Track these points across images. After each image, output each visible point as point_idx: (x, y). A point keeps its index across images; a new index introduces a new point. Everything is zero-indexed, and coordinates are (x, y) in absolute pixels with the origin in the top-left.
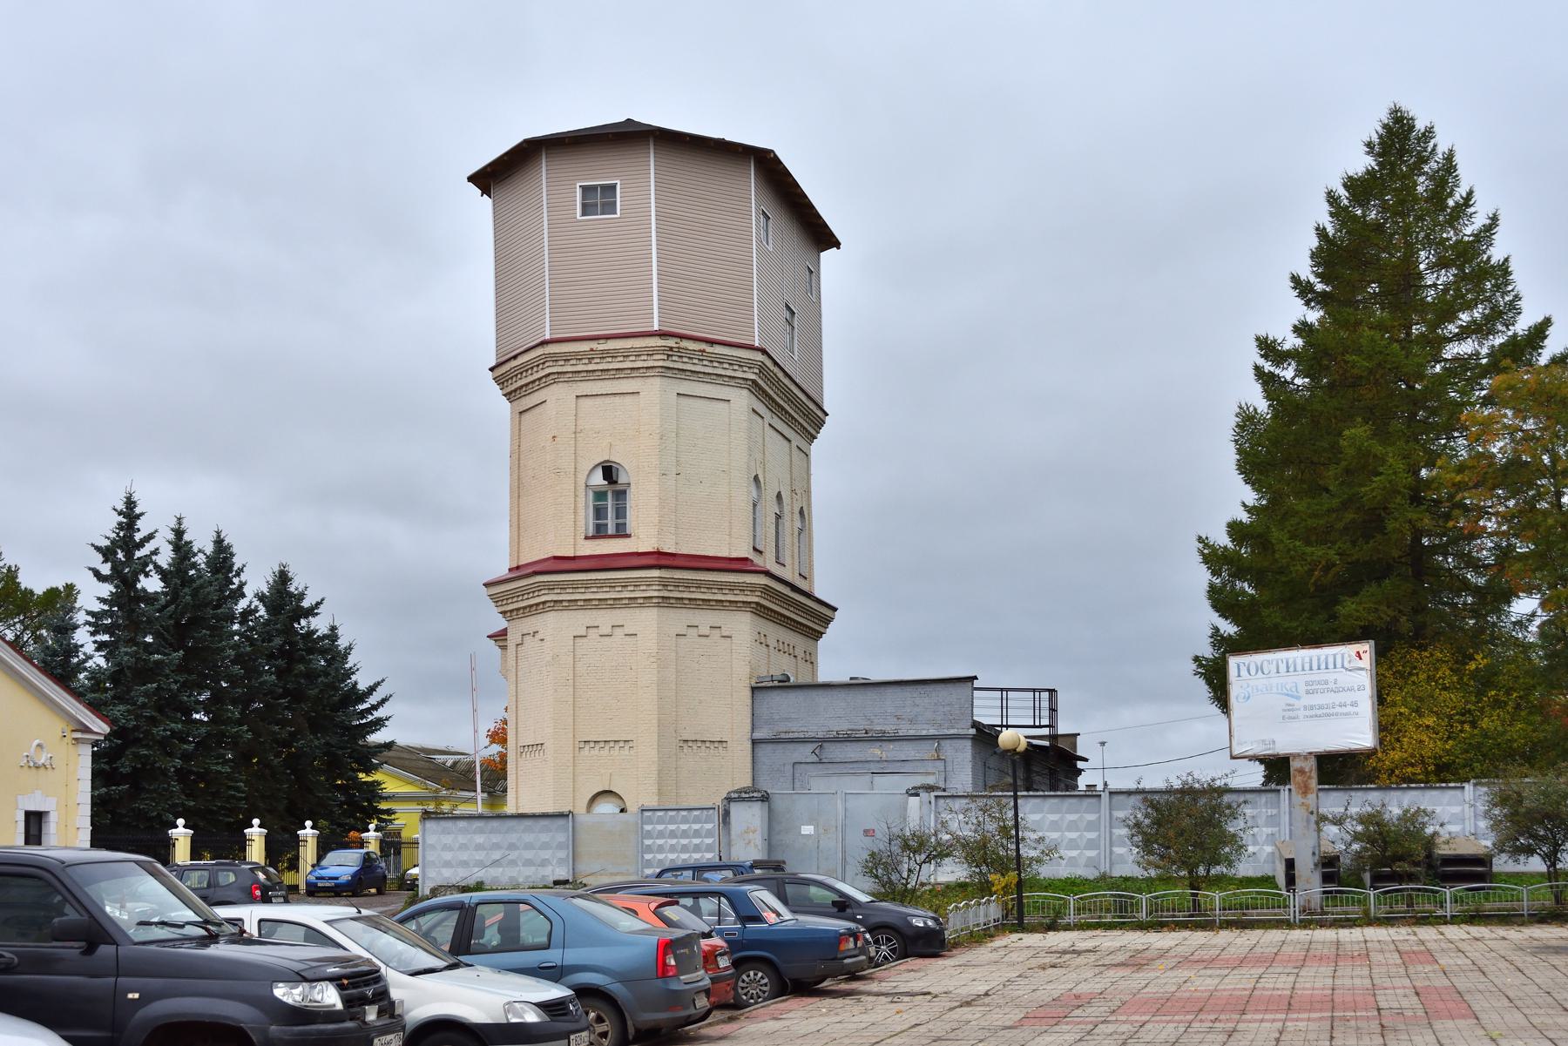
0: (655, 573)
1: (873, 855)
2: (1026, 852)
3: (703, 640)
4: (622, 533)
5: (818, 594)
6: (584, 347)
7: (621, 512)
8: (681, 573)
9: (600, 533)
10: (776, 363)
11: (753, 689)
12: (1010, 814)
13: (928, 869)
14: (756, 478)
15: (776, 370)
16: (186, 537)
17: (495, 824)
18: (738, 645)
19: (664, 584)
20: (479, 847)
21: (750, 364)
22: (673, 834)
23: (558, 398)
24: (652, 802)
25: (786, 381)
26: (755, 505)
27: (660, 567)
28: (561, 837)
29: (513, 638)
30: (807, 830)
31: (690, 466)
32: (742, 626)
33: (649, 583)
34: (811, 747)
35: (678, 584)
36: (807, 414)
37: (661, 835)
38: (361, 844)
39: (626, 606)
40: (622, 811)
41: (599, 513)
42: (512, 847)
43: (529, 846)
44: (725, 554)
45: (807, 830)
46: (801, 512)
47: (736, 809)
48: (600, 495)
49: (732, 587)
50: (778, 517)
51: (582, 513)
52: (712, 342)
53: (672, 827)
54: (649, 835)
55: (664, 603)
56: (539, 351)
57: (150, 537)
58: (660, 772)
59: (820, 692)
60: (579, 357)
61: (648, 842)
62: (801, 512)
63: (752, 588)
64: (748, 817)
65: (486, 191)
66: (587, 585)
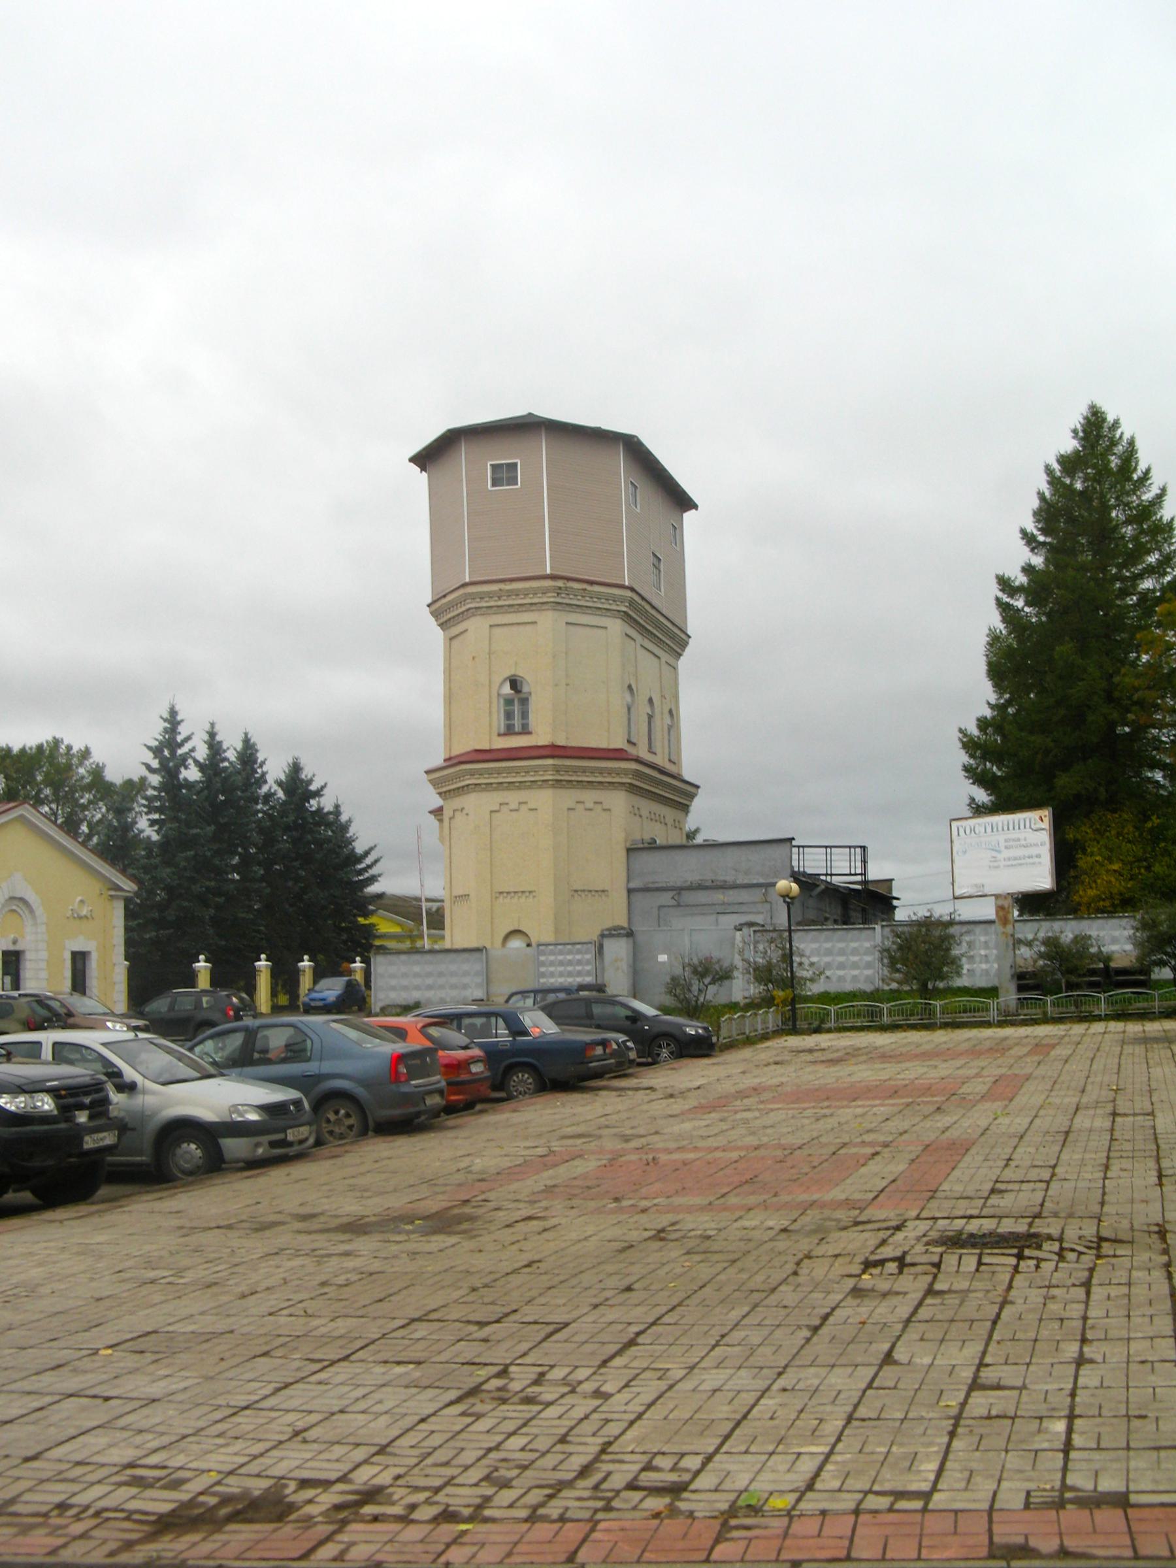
0: (550, 762)
1: (673, 979)
2: (801, 973)
3: (588, 813)
4: (525, 731)
5: (687, 778)
7: (525, 715)
8: (572, 763)
9: (509, 731)
10: (643, 598)
11: (629, 850)
12: (788, 946)
13: (712, 989)
14: (630, 687)
15: (643, 603)
16: (218, 738)
17: (417, 957)
18: (616, 816)
19: (557, 769)
20: (417, 975)
21: (622, 600)
22: (561, 963)
23: (476, 626)
24: (549, 937)
25: (653, 612)
26: (629, 709)
27: (552, 757)
28: (478, 967)
29: (447, 813)
30: (663, 958)
31: (578, 680)
32: (619, 801)
33: (545, 769)
34: (671, 894)
35: (568, 769)
36: (673, 637)
37: (552, 964)
38: (350, 972)
39: (530, 788)
40: (529, 945)
41: (509, 715)
42: (441, 974)
44: (604, 745)
45: (663, 958)
46: (670, 712)
47: (609, 944)
48: (509, 702)
49: (610, 772)
50: (650, 717)
51: (495, 716)
52: (592, 583)
53: (560, 958)
54: (543, 964)
55: (558, 784)
56: (461, 592)
57: (188, 739)
59: (678, 852)
60: (490, 595)
61: (543, 969)
62: (670, 712)
63: (626, 772)
64: (618, 949)
65: (423, 468)
66: (499, 772)
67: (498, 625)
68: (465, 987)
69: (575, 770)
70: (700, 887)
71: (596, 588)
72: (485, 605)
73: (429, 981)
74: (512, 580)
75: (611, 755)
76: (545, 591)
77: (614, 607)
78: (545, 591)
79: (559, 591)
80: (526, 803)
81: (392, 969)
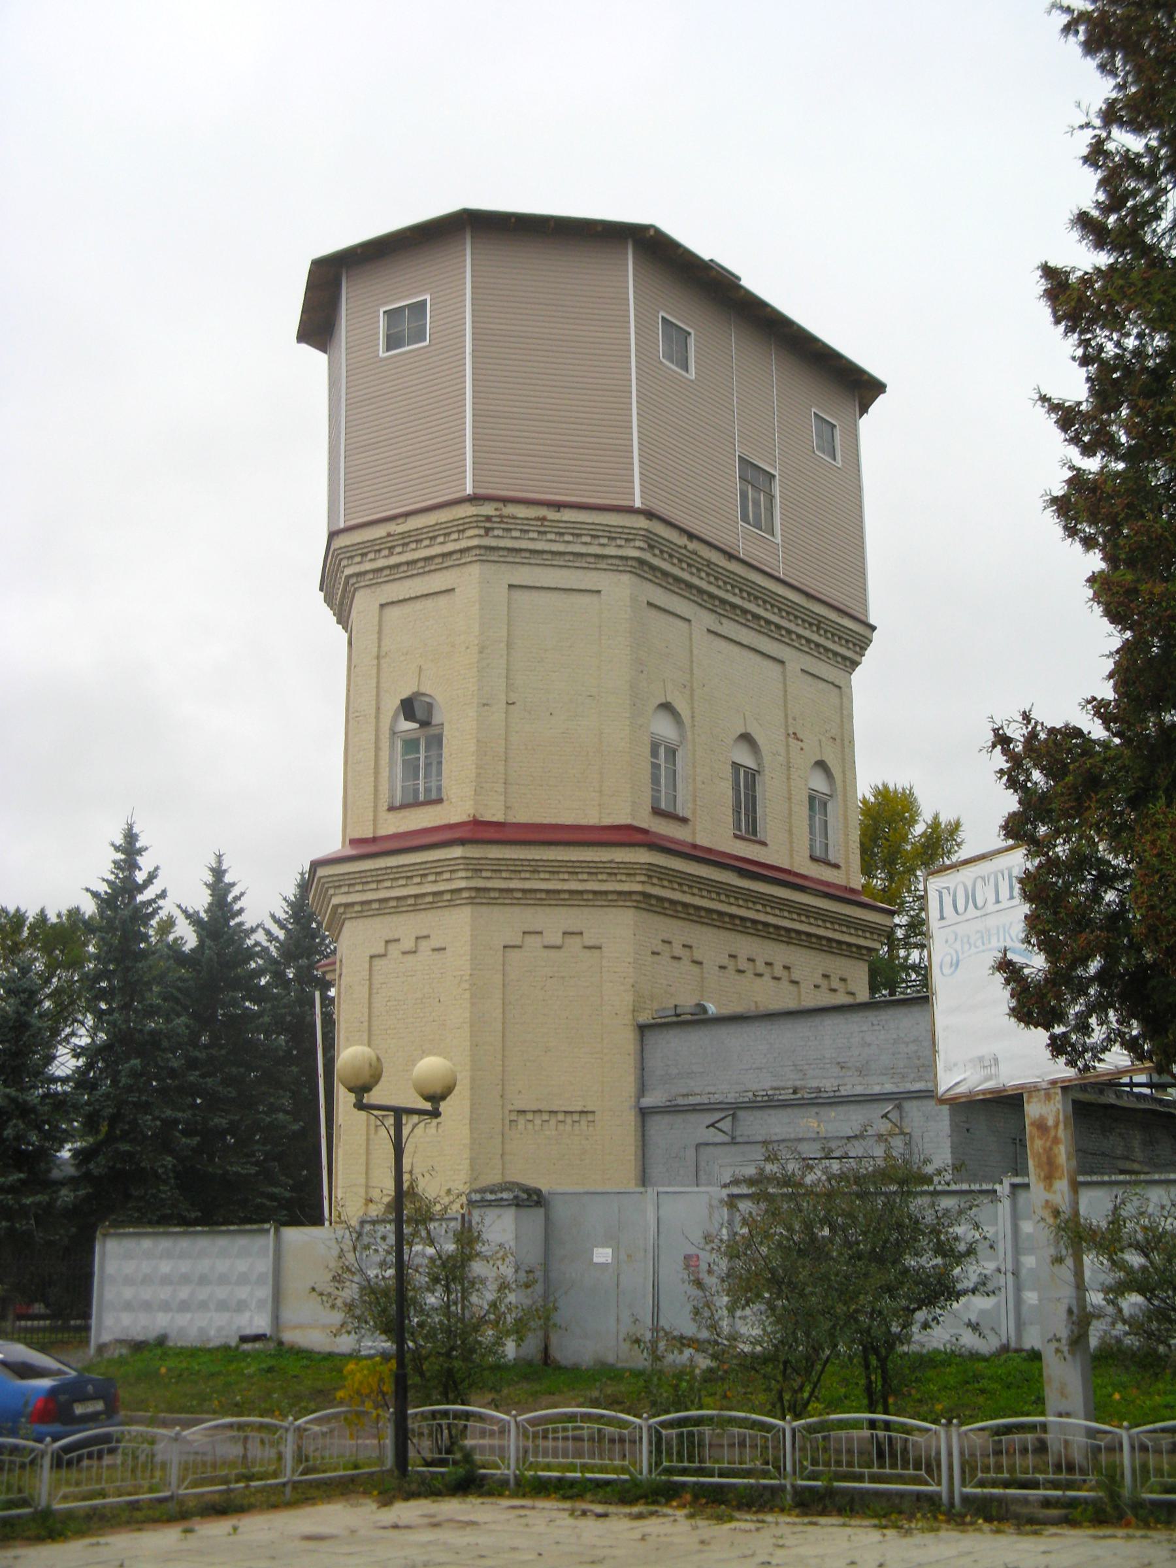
0: (457, 852)
3: (553, 953)
6: (379, 532)
9: (412, 803)
10: (691, 536)
16: (228, 879)
20: (166, 1280)
25: (733, 566)
27: (462, 842)
30: (603, 1255)
32: (620, 932)
35: (498, 867)
41: (411, 769)
42: (203, 1280)
43: (223, 1280)
45: (603, 1255)
48: (411, 745)
52: (558, 506)
55: (480, 897)
58: (473, 1161)
63: (630, 870)
67: (393, 603)
68: (241, 1306)
69: (516, 868)
70: (768, 1103)
71: (568, 515)
72: (368, 566)
73: (184, 1293)
74: (407, 515)
75: (606, 837)
76: (461, 527)
77: (611, 551)
78: (461, 527)
79: (487, 525)
80: (427, 937)
81: (129, 1267)
